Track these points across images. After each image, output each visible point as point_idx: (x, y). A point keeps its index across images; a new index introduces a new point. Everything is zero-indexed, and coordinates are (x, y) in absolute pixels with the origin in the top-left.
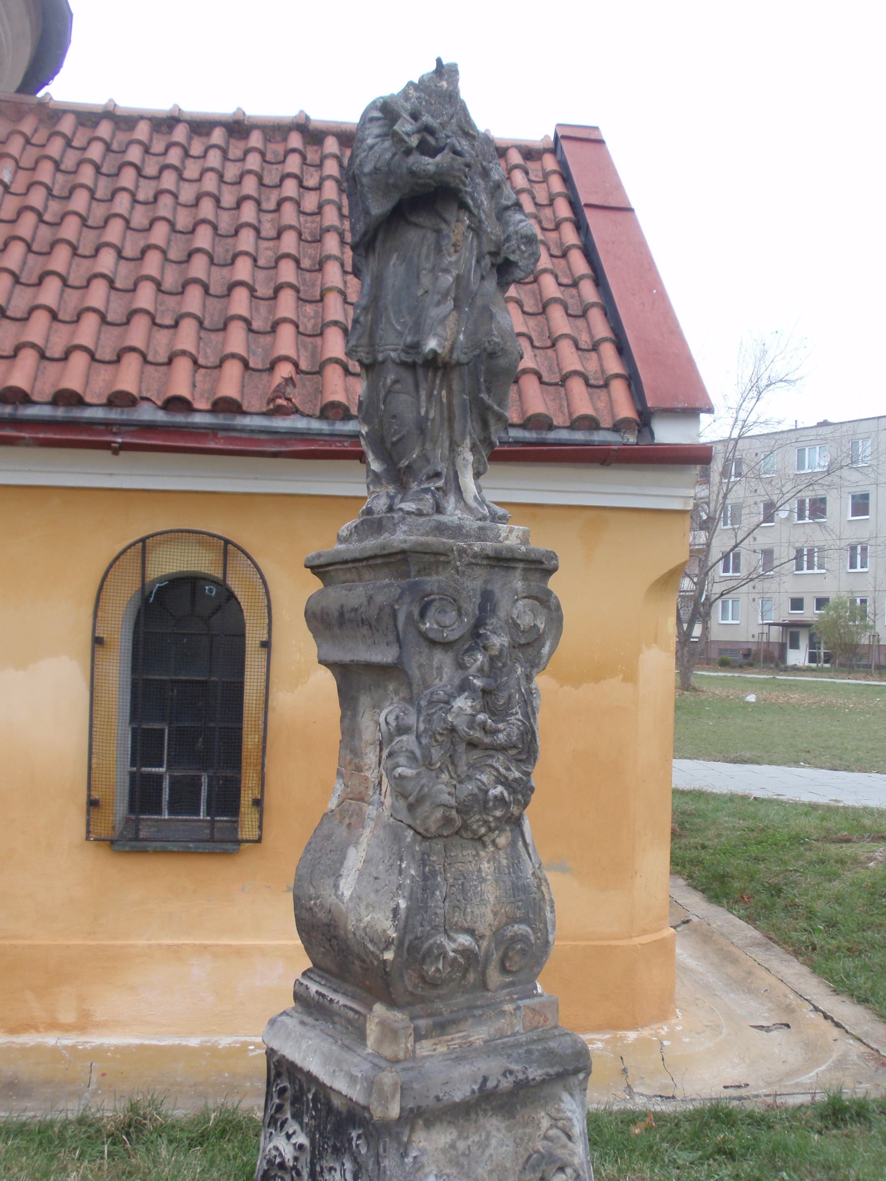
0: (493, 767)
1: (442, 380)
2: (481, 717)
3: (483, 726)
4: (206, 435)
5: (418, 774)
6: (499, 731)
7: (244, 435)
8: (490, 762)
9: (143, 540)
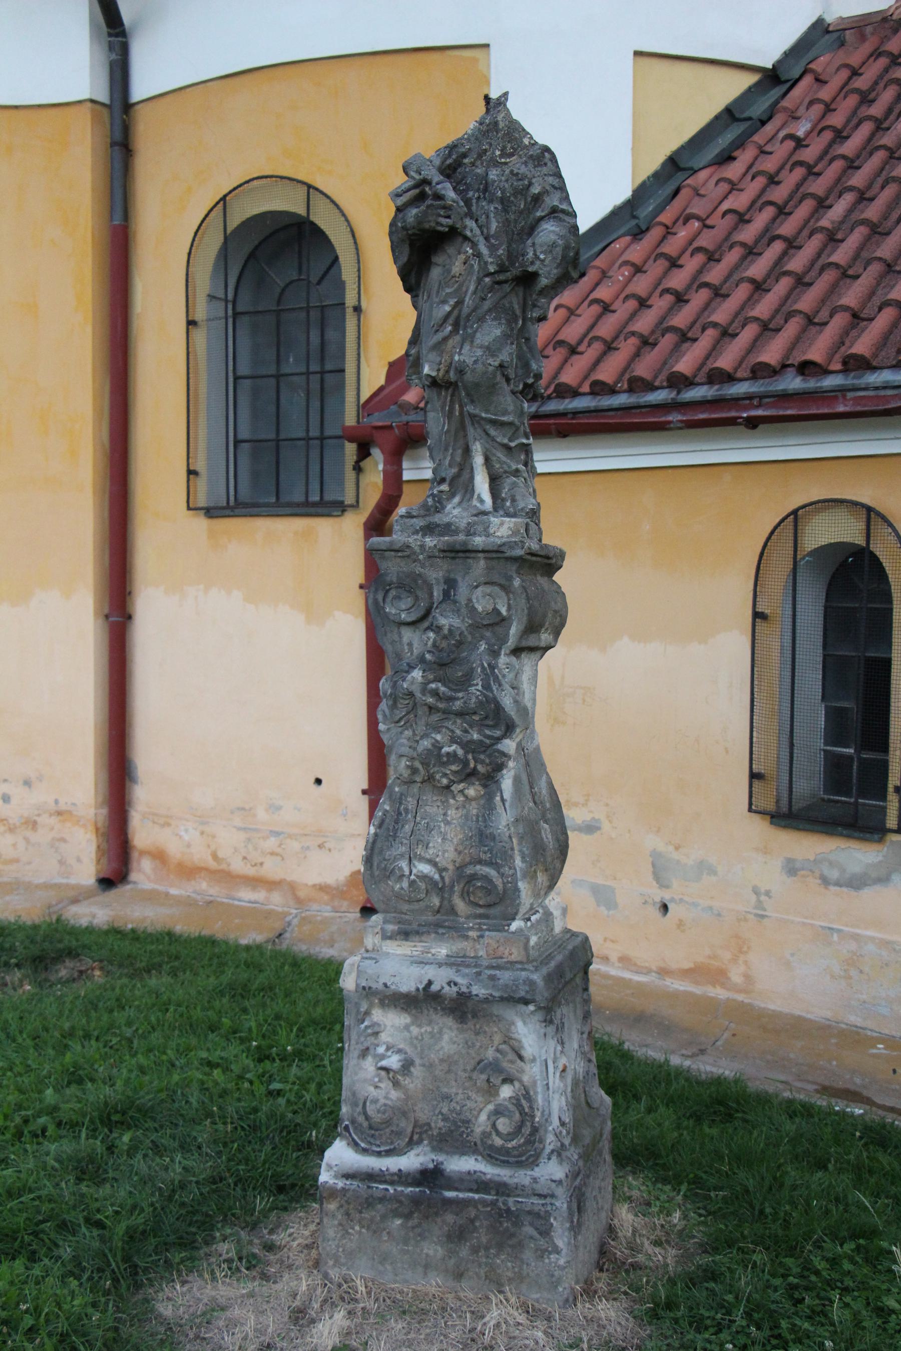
0: (447, 728)
1: (452, 396)
2: (433, 686)
3: (435, 693)
4: (836, 397)
5: (388, 729)
6: (458, 699)
7: (871, 393)
8: (446, 724)
9: (795, 512)
